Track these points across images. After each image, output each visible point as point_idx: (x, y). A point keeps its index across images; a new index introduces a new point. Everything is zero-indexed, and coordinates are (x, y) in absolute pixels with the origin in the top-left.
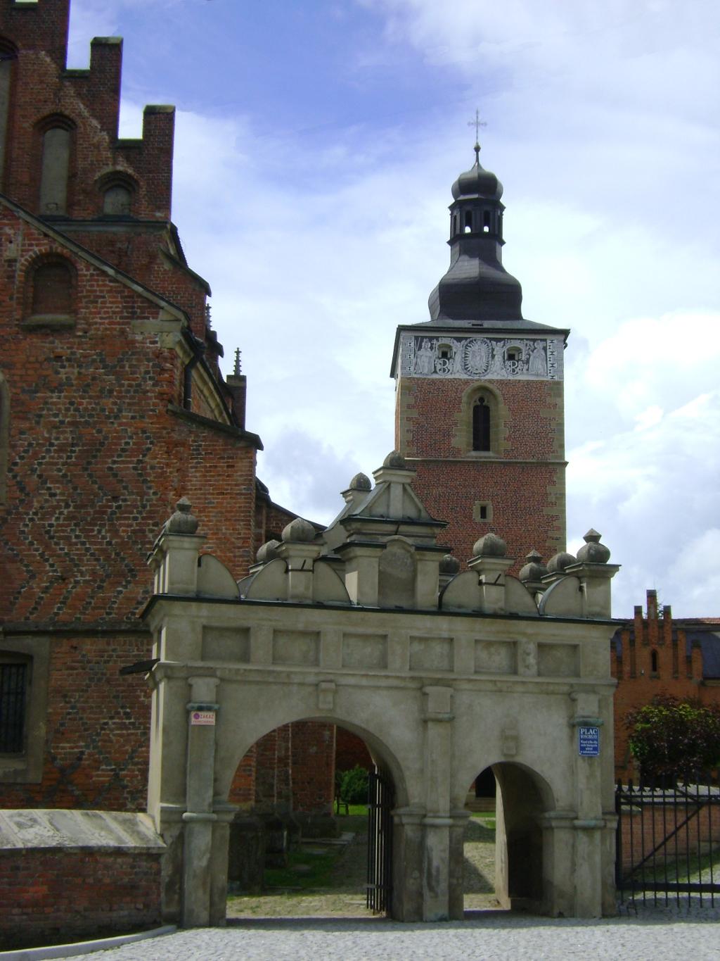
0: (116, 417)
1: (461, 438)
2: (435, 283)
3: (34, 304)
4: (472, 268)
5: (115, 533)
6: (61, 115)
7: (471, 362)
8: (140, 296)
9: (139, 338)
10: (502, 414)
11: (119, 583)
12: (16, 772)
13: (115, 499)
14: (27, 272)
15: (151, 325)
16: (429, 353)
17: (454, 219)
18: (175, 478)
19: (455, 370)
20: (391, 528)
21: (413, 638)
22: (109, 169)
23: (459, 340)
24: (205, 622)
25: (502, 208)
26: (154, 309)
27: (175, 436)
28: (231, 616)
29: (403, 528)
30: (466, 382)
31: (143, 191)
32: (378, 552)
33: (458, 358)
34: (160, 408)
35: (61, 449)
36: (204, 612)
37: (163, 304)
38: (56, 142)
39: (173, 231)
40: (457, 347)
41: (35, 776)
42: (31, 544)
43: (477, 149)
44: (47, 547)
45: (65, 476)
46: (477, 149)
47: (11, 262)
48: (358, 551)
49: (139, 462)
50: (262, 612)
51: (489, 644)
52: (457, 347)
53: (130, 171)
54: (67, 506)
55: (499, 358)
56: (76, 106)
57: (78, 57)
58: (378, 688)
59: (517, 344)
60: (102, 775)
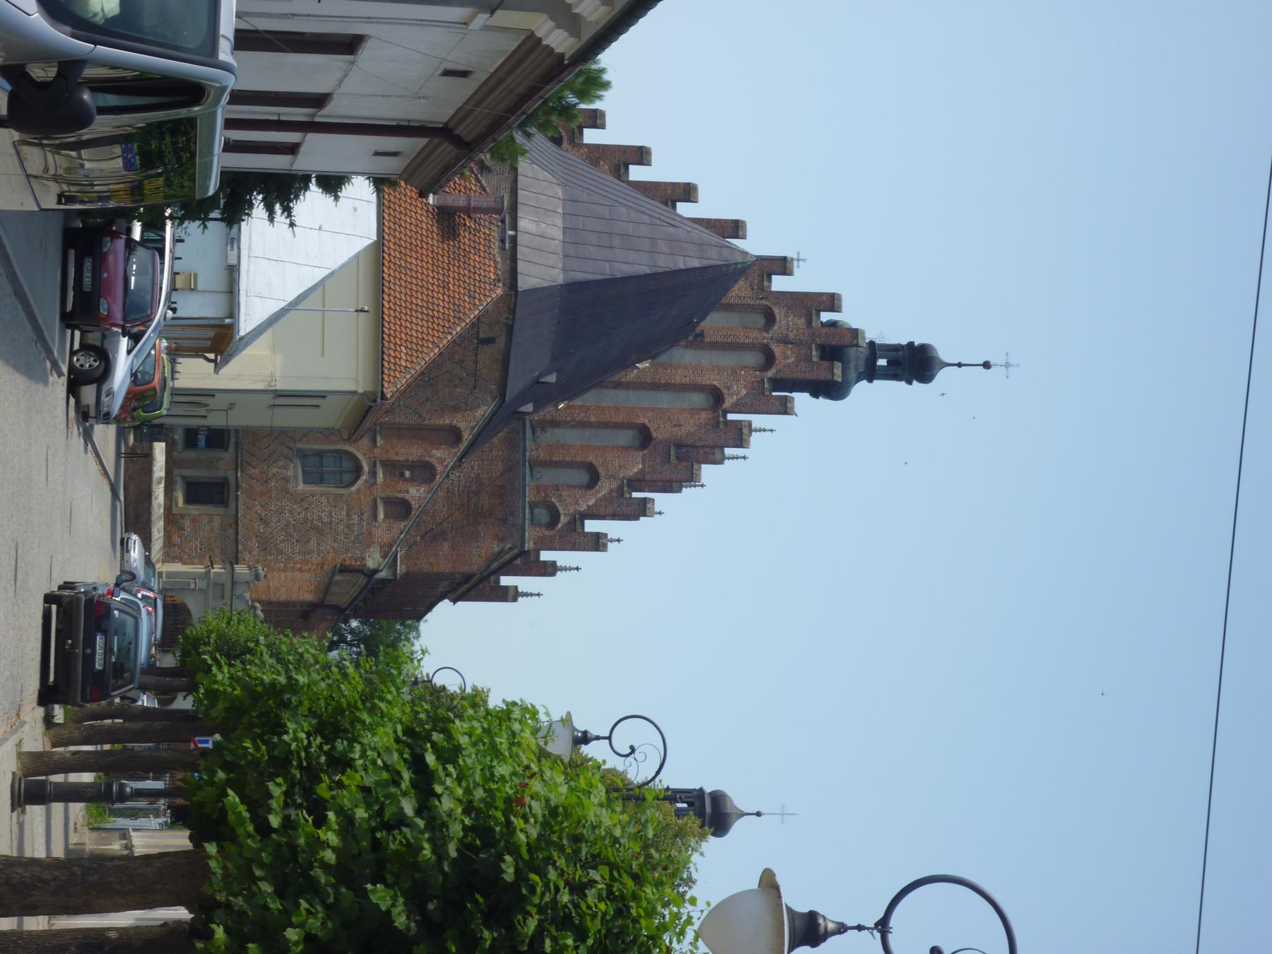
3: (388, 501)
5: (282, 542)
6: (598, 479)
15: (377, 556)
18: (306, 567)
26: (384, 557)
27: (326, 567)
28: (228, 594)
31: (547, 533)
35: (320, 518)
36: (229, 584)
38: (583, 477)
41: (175, 511)
43: (758, 814)
46: (758, 814)
47: (407, 492)
53: (560, 526)
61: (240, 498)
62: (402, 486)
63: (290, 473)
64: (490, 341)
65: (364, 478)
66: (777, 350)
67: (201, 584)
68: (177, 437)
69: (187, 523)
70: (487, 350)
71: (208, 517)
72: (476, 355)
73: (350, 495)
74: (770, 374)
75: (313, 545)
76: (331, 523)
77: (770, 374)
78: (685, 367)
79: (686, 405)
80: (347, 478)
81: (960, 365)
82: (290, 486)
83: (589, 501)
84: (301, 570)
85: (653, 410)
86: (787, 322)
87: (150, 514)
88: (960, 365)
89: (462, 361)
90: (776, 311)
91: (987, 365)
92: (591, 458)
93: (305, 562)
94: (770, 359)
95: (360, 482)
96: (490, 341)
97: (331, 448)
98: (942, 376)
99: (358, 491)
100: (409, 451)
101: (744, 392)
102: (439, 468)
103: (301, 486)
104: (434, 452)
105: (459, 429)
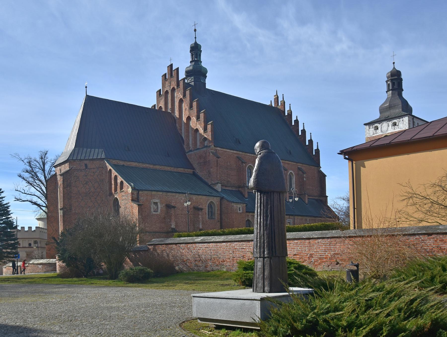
7: (383, 129)
55: (390, 126)
64: (86, 165)
66: (172, 87)
70: (89, 166)
74: (176, 87)
77: (176, 87)
88: (195, 38)
96: (86, 165)
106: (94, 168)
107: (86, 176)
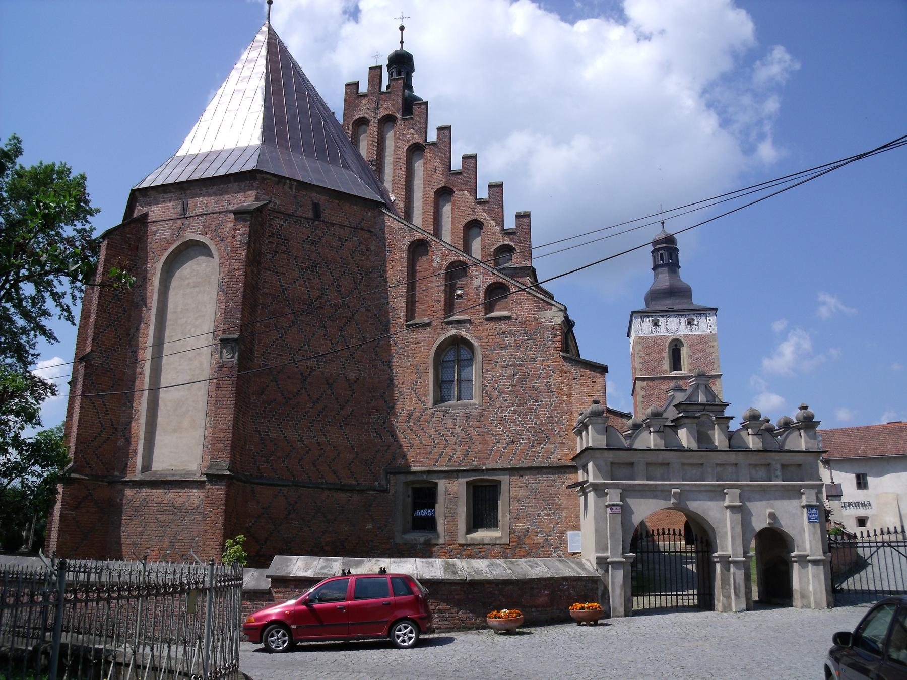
0: (535, 361)
1: (666, 366)
2: (646, 290)
3: (489, 308)
4: (665, 280)
6: (476, 220)
8: (542, 300)
9: (543, 320)
10: (684, 351)
11: (542, 443)
12: (497, 538)
13: (537, 401)
14: (486, 292)
15: (549, 313)
16: (648, 324)
17: (654, 257)
18: (566, 389)
19: (662, 331)
20: (702, 407)
21: (717, 465)
22: (501, 243)
23: (662, 316)
24: (611, 460)
25: (678, 250)
27: (565, 368)
29: (707, 408)
30: (668, 337)
32: (696, 420)
33: (663, 325)
34: (557, 355)
35: (509, 377)
36: (610, 456)
37: (554, 303)
39: (534, 270)
40: (662, 321)
42: (497, 425)
44: (505, 426)
45: (511, 391)
47: (478, 288)
48: (686, 420)
49: (548, 382)
50: (640, 454)
51: (756, 466)
52: (662, 321)
53: (512, 244)
54: (513, 406)
55: (683, 324)
56: (482, 215)
57: (483, 193)
58: (700, 491)
59: (691, 316)
60: (539, 539)
61: (490, 467)
62: (472, 294)
63: (461, 412)
64: (316, 208)
65: (463, 334)
66: (382, 113)
67: (614, 497)
68: (422, 540)
69: (520, 526)
70: (326, 213)
71: (513, 495)
72: (333, 224)
73: (482, 346)
74: (399, 116)
75: (541, 384)
76: (514, 366)
77: (399, 116)
78: (395, 170)
79: (422, 169)
80: (464, 354)
81: (402, 42)
82: (475, 412)
83: (491, 225)
84: (569, 396)
85: (424, 188)
86: (364, 110)
87: (507, 582)
88: (402, 42)
89: (340, 239)
90: (356, 117)
91: (402, 28)
92: (461, 227)
93: (560, 390)
94: (389, 120)
95: (468, 337)
96: (316, 208)
97: (432, 371)
98: (407, 48)
99: (479, 338)
100: (433, 292)
101: (411, 131)
102: (452, 258)
103: (475, 401)
104: (435, 264)
105: (412, 243)
106: (342, 226)
107: (314, 243)
